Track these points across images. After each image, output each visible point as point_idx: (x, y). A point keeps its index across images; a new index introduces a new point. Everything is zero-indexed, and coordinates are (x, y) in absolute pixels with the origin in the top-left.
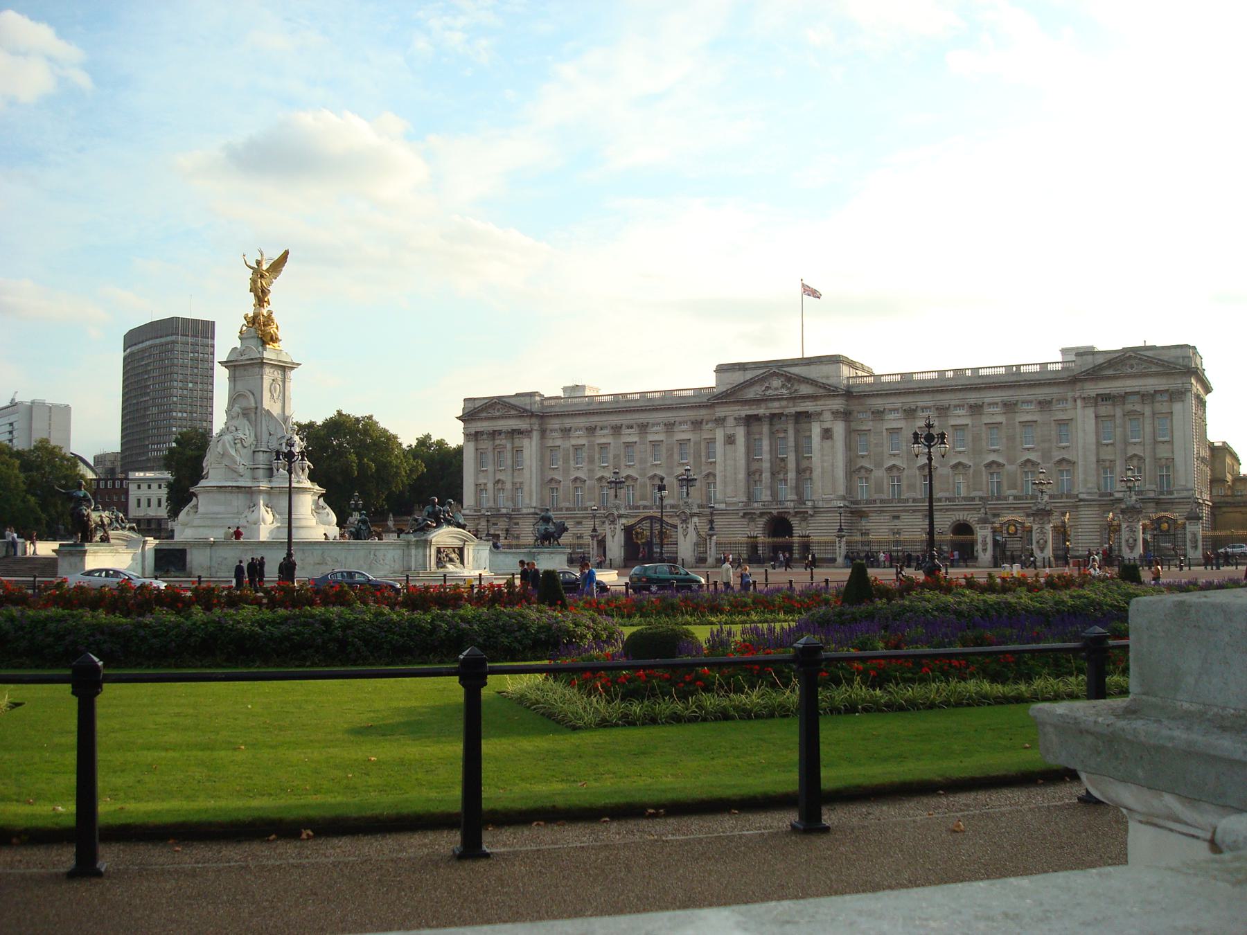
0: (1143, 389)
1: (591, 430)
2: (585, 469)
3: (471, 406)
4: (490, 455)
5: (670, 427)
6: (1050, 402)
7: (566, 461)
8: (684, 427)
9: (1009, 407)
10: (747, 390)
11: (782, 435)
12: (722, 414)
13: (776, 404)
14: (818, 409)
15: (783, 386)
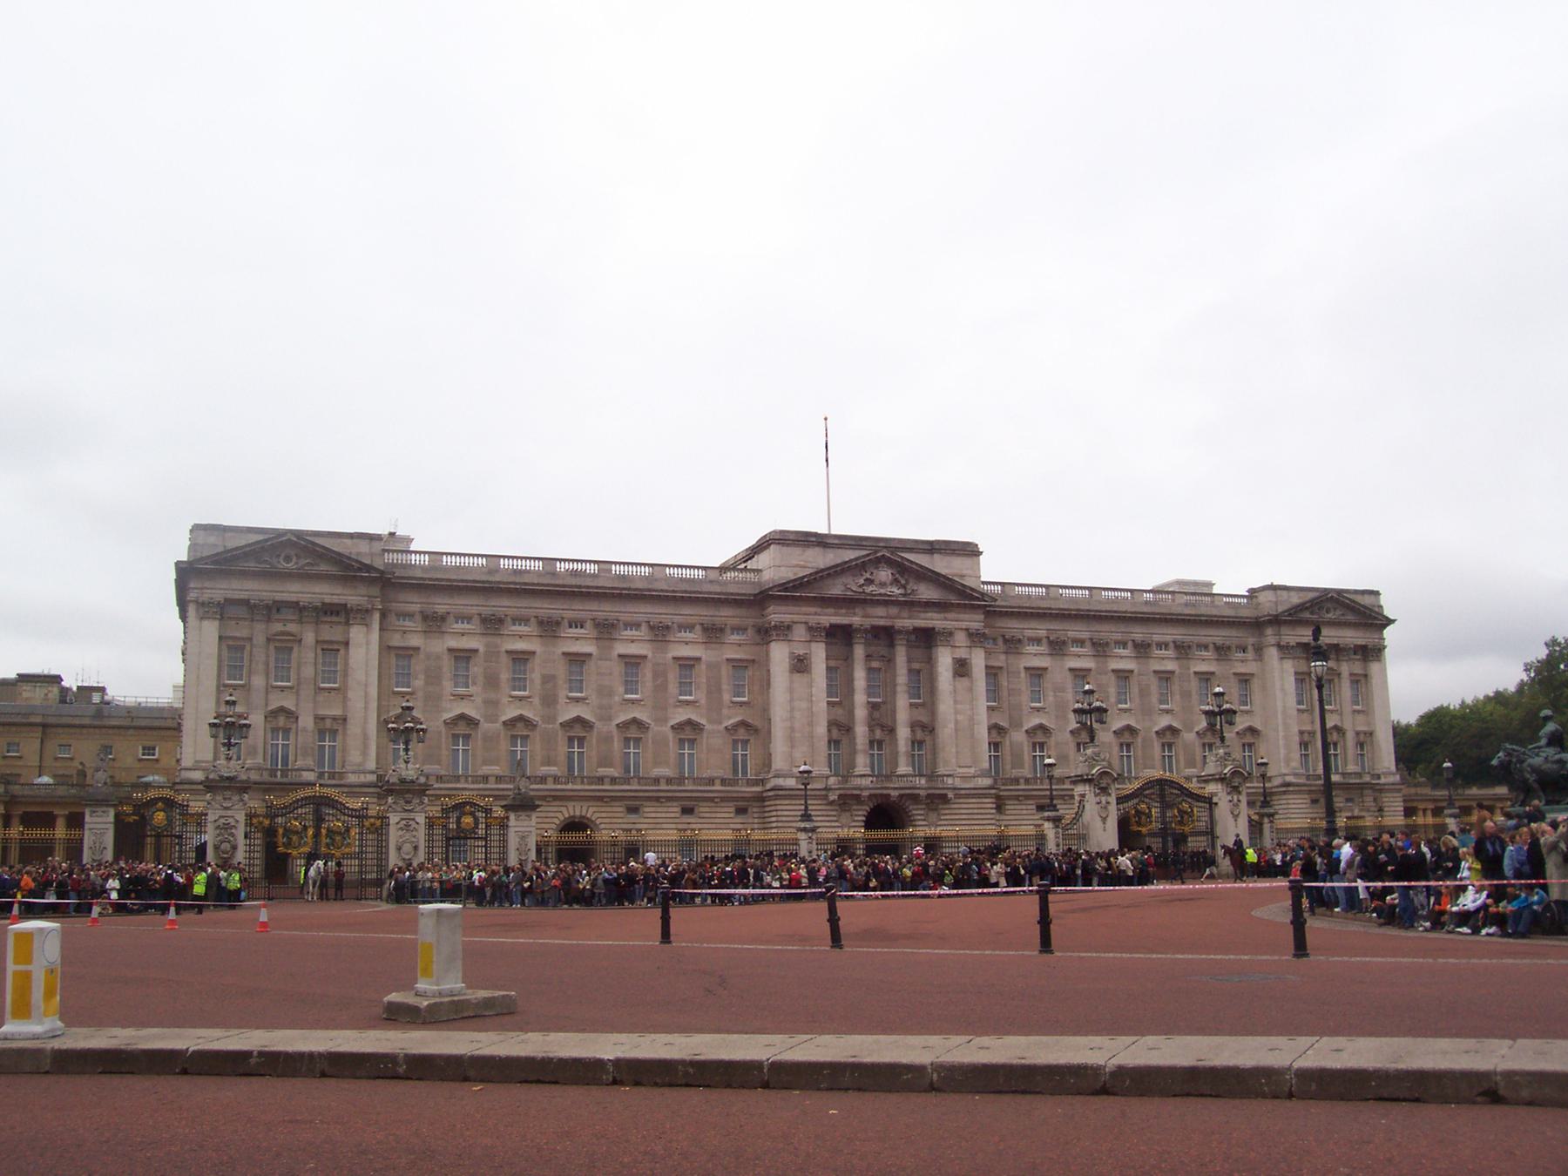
0: (1341, 641)
1: (493, 624)
2: (479, 700)
3: (212, 540)
4: (260, 655)
5: (660, 632)
6: (1229, 648)
7: (433, 678)
8: (689, 636)
9: (1183, 650)
10: (829, 582)
11: (875, 664)
12: (787, 618)
13: (880, 611)
14: (949, 625)
15: (895, 581)
